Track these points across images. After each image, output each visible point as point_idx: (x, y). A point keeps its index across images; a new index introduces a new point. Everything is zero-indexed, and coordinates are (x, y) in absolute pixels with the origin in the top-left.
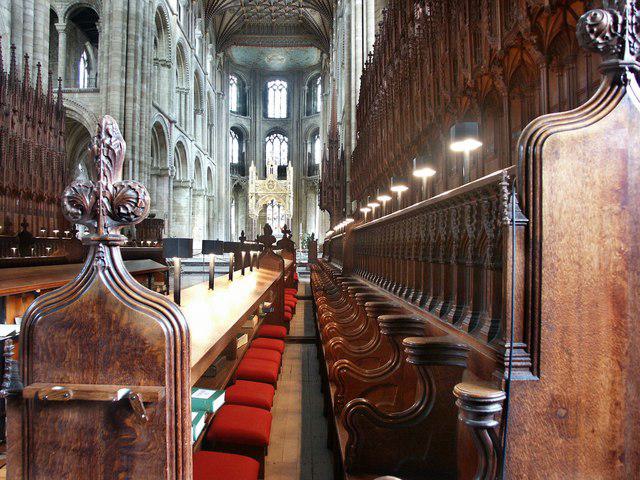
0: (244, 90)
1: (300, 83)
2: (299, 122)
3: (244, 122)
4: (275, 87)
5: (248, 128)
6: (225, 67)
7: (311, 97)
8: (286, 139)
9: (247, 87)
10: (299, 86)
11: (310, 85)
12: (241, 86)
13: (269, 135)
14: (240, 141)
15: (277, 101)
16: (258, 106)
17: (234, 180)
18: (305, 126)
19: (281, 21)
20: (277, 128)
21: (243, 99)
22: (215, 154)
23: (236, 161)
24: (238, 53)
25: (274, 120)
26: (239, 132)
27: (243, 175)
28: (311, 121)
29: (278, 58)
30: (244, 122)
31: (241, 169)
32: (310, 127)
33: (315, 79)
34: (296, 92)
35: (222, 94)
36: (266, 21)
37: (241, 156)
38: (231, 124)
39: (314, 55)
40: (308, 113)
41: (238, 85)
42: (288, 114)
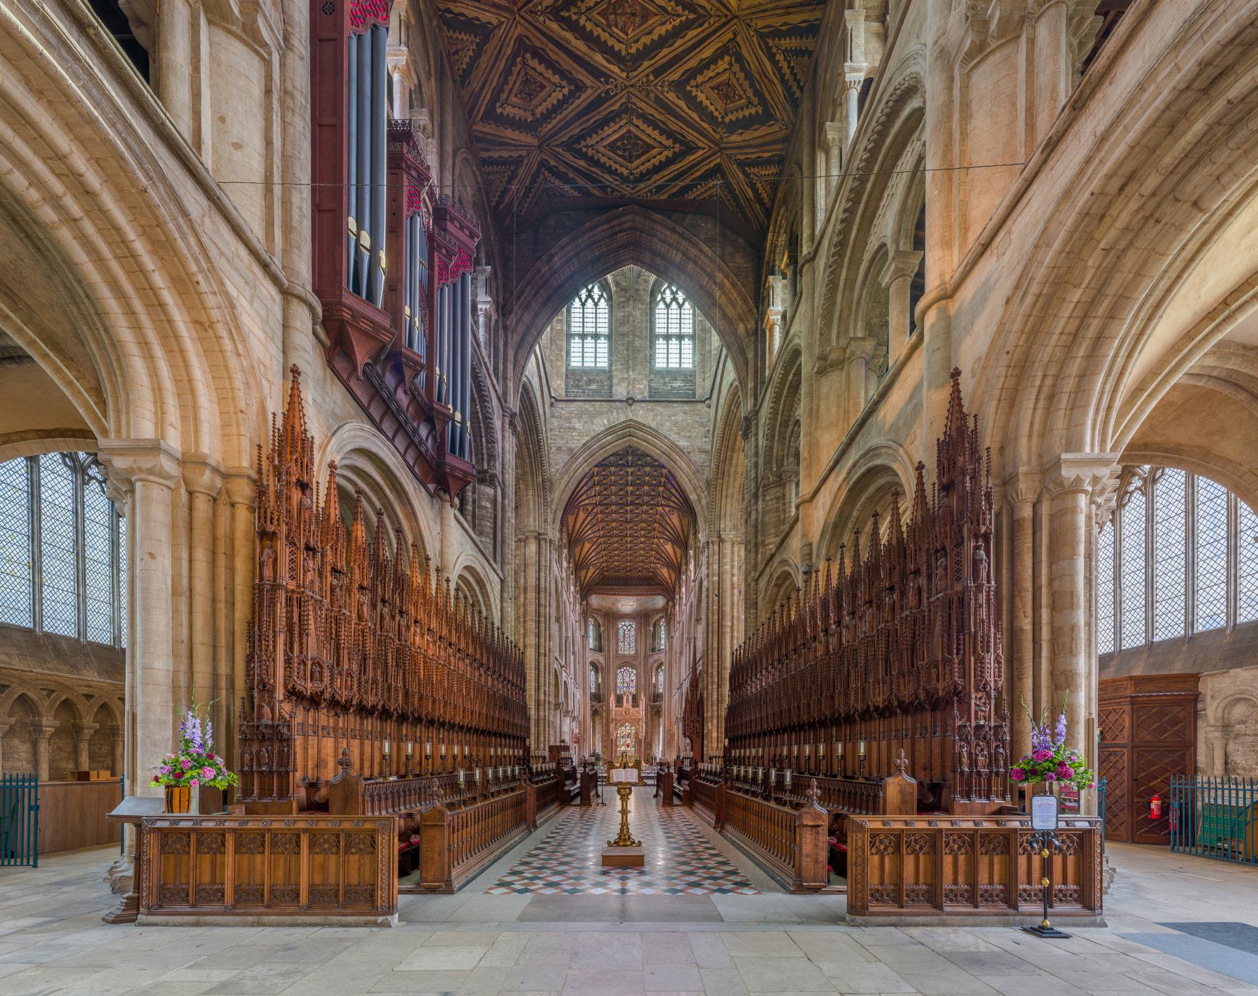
1: (647, 625)
2: (646, 658)
3: (600, 658)
6: (586, 614)
7: (654, 636)
11: (654, 626)
14: (597, 672)
15: (627, 638)
18: (651, 661)
19: (634, 574)
20: (626, 662)
21: (599, 637)
22: (552, 672)
24: (595, 600)
25: (625, 656)
26: (595, 666)
28: (656, 657)
29: (627, 604)
30: (600, 658)
31: (597, 697)
33: (658, 620)
35: (585, 637)
36: (622, 574)
37: (598, 686)
39: (660, 601)
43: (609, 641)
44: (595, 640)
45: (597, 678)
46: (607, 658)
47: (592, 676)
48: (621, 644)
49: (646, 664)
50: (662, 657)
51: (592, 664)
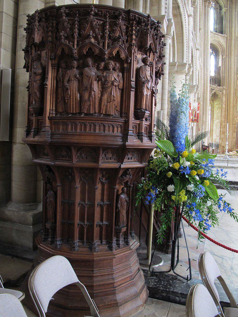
0: (220, 13)
3: (221, 40)
9: (224, 10)
12: (219, 8)
17: (212, 90)
21: (220, 20)
23: (213, 74)
26: (215, 49)
27: (219, 85)
37: (218, 70)
38: (210, 41)
41: (215, 9)
44: (216, 23)
46: (229, 40)
47: (212, 60)
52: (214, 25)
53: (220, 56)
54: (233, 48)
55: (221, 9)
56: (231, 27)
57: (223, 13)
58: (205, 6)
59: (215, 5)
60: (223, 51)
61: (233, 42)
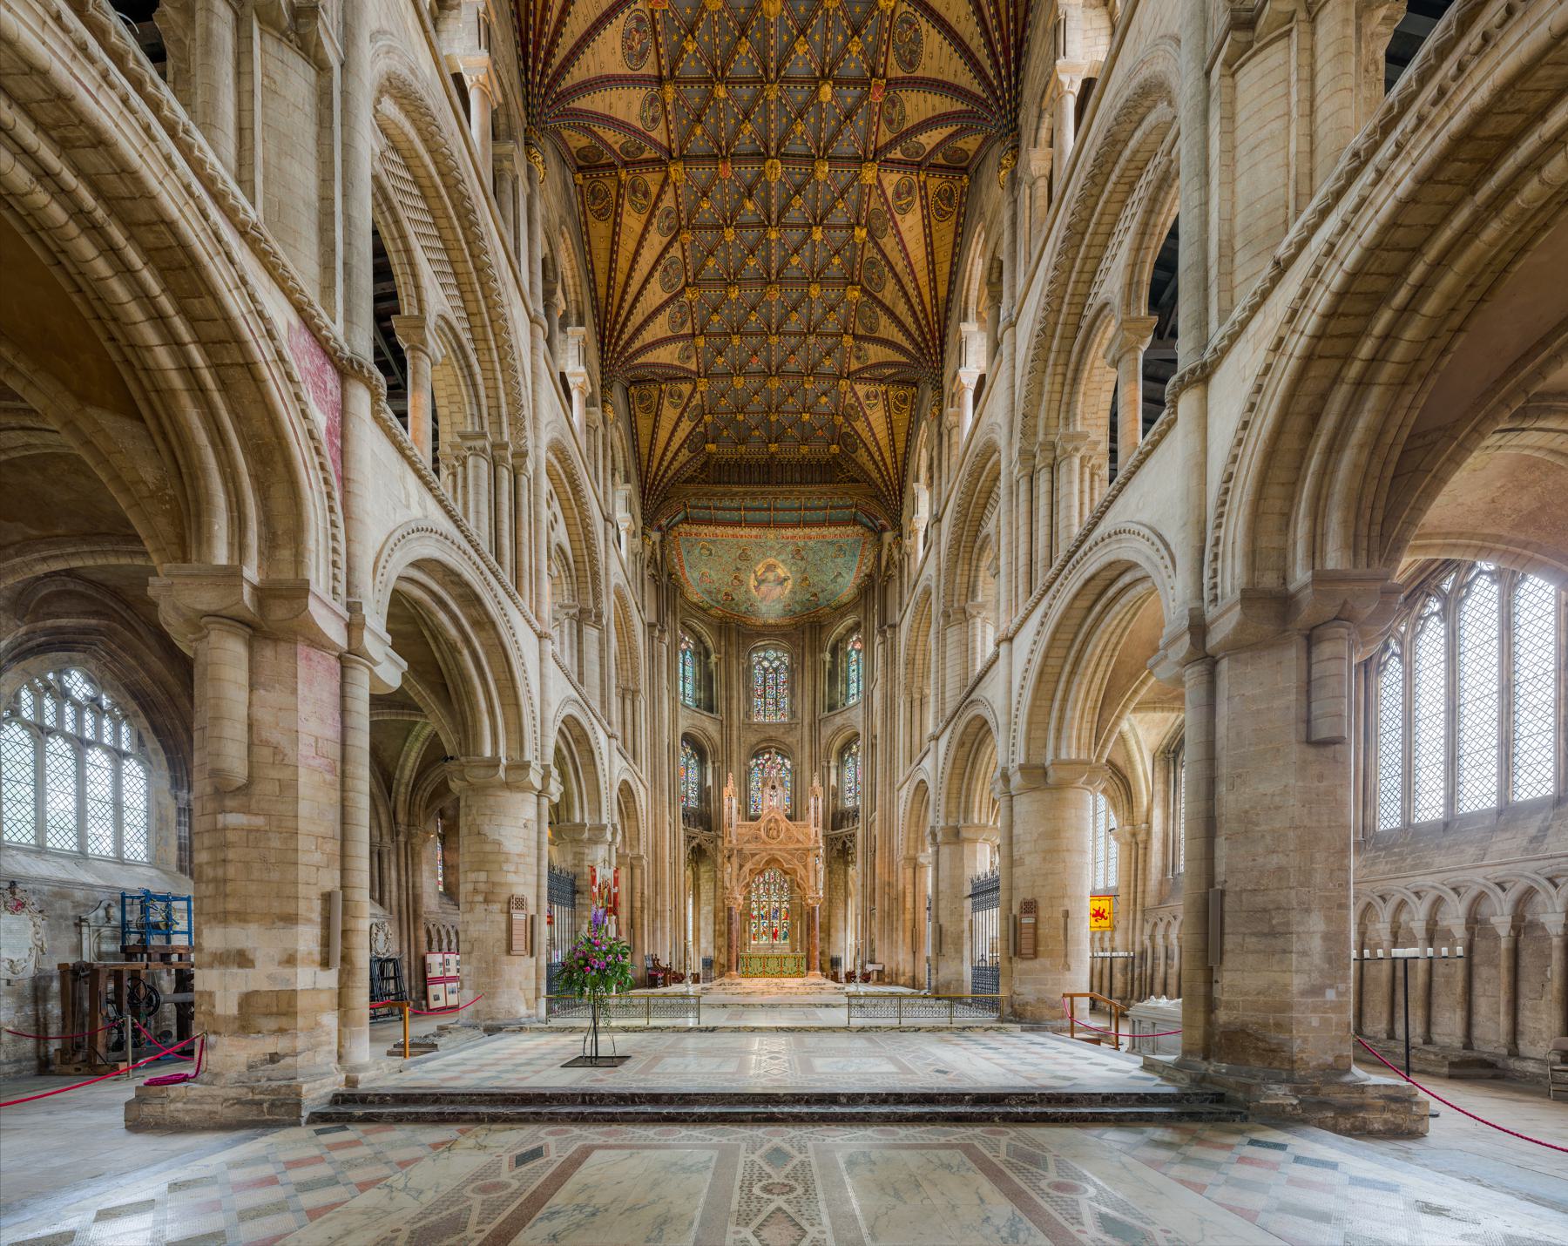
0: (707, 665)
1: (817, 648)
4: (766, 664)
5: (716, 736)
8: (788, 763)
9: (713, 658)
10: (813, 654)
13: (756, 755)
16: (735, 694)
18: (826, 732)
21: (706, 680)
28: (839, 720)
32: (839, 730)
34: (808, 662)
40: (832, 707)
42: (793, 713)
43: (728, 687)
45: (703, 776)
46: (725, 727)
48: (758, 702)
49: (814, 740)
50: (856, 719)
51: (687, 738)
52: (694, 690)
53: (710, 763)
54: (735, 747)
55: (708, 656)
56: (729, 699)
57: (713, 666)
58: (652, 638)
59: (696, 645)
60: (715, 752)
61: (735, 733)
